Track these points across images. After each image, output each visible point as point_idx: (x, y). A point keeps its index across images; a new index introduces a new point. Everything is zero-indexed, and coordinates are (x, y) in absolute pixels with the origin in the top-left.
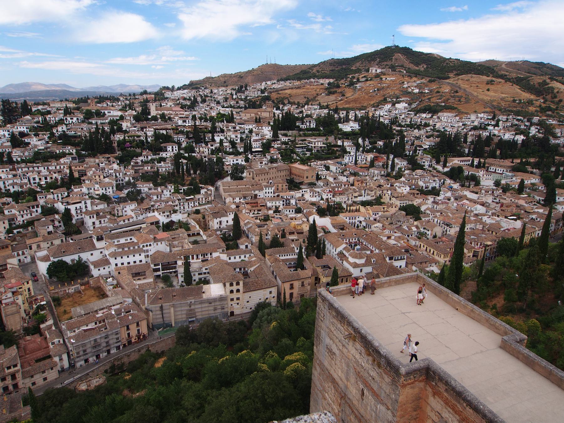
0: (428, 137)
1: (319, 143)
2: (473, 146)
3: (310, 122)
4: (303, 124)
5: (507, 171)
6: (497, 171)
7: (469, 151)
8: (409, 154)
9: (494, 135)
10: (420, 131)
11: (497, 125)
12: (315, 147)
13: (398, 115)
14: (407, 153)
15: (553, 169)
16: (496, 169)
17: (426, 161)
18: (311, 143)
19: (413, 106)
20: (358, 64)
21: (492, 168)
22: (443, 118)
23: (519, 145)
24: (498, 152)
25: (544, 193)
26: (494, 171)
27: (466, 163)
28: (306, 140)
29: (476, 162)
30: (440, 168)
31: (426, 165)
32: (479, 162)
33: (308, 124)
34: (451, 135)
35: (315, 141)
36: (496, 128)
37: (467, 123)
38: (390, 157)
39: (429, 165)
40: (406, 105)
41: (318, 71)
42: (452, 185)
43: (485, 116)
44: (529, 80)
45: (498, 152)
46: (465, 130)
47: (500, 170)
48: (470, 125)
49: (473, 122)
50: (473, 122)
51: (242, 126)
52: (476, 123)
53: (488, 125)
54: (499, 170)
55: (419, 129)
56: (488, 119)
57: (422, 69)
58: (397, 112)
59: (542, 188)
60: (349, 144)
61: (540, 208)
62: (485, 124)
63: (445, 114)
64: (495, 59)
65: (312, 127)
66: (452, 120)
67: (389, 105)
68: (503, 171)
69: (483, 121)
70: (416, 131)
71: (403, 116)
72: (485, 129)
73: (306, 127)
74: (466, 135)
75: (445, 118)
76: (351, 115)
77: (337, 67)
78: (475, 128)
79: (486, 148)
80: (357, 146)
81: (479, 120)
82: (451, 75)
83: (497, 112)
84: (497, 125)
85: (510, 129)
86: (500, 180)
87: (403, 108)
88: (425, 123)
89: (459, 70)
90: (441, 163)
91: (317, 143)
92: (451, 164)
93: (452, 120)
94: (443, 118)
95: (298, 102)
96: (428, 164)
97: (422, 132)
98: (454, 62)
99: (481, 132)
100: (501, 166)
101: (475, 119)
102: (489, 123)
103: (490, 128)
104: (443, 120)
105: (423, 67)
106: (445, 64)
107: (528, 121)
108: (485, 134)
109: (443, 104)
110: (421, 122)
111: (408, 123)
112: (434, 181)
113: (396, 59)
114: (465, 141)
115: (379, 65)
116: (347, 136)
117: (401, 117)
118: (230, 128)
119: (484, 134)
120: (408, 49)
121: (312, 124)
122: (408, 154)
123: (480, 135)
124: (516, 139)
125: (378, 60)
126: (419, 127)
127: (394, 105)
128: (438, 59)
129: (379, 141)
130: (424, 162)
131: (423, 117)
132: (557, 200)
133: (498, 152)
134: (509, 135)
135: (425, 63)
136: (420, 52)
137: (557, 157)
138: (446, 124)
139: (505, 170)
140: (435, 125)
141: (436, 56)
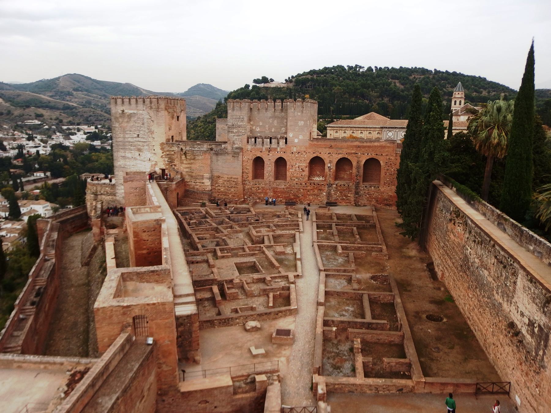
15: (11, 182)
25: (8, 207)
59: (5, 203)
137: (12, 170)
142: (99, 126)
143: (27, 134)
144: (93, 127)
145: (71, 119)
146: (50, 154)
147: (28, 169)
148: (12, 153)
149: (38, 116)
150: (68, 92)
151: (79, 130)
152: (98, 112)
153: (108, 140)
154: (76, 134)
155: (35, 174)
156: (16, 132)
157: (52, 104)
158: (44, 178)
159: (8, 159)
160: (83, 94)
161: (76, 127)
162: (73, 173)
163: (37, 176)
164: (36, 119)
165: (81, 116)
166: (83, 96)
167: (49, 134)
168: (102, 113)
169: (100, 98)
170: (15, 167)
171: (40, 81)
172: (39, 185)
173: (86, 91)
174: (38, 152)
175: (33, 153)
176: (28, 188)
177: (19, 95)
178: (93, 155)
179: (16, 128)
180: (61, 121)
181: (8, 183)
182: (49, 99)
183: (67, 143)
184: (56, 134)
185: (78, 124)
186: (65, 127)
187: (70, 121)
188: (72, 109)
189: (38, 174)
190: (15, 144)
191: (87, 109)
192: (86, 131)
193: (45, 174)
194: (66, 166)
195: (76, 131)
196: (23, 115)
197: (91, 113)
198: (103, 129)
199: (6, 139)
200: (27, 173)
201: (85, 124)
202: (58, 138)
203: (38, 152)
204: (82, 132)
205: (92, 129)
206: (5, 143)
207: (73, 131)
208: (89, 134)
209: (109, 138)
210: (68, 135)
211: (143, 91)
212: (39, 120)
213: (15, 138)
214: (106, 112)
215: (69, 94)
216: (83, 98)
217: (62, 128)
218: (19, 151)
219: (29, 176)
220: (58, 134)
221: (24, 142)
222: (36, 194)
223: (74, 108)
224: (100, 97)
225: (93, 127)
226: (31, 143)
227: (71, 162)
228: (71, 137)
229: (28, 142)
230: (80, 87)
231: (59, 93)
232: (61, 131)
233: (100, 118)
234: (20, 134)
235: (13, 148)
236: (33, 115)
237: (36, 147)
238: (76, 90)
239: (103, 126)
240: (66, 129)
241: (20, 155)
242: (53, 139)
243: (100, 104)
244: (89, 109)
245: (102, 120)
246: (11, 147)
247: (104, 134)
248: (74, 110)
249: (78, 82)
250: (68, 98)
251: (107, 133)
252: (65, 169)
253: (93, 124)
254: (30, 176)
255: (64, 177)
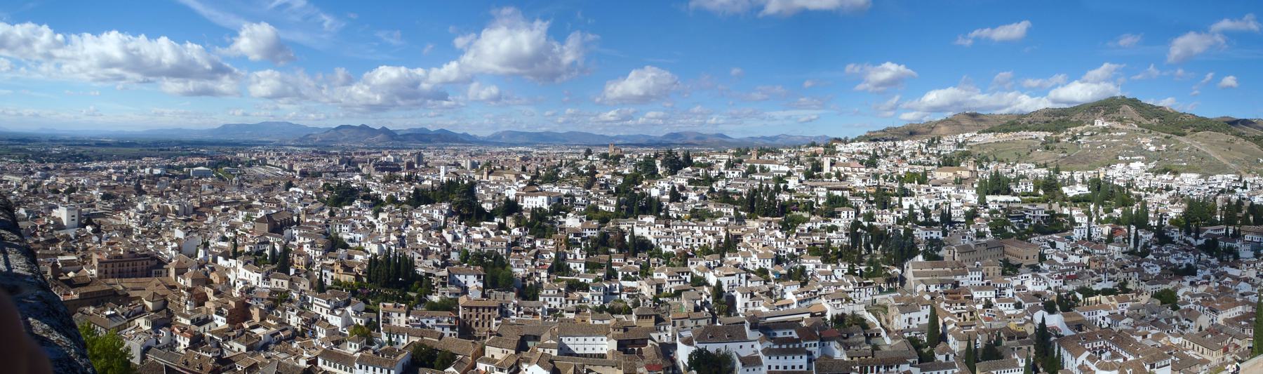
1: (1040, 212)
2: (1224, 212)
3: (1026, 184)
4: (1017, 187)
7: (1221, 218)
9: (1244, 199)
11: (1245, 187)
12: (1034, 217)
13: (1134, 177)
22: (1186, 179)
24: (1251, 218)
26: (1250, 240)
33: (1024, 187)
35: (1034, 208)
36: (1245, 190)
40: (1143, 165)
49: (1219, 184)
50: (1219, 184)
51: (938, 188)
52: (1223, 186)
53: (1236, 187)
56: (1234, 180)
70: (1158, 195)
72: (1233, 192)
78: (1222, 191)
84: (1245, 187)
87: (1139, 168)
88: (1167, 186)
90: (1193, 234)
91: (1036, 212)
94: (1186, 179)
99: (1230, 196)
103: (1238, 190)
108: (1234, 198)
109: (1185, 164)
110: (1162, 185)
111: (1147, 186)
116: (1076, 200)
117: (1138, 179)
118: (922, 190)
119: (1233, 198)
121: (1028, 188)
126: (1160, 191)
127: (1127, 163)
130: (1173, 234)
140: (1178, 188)
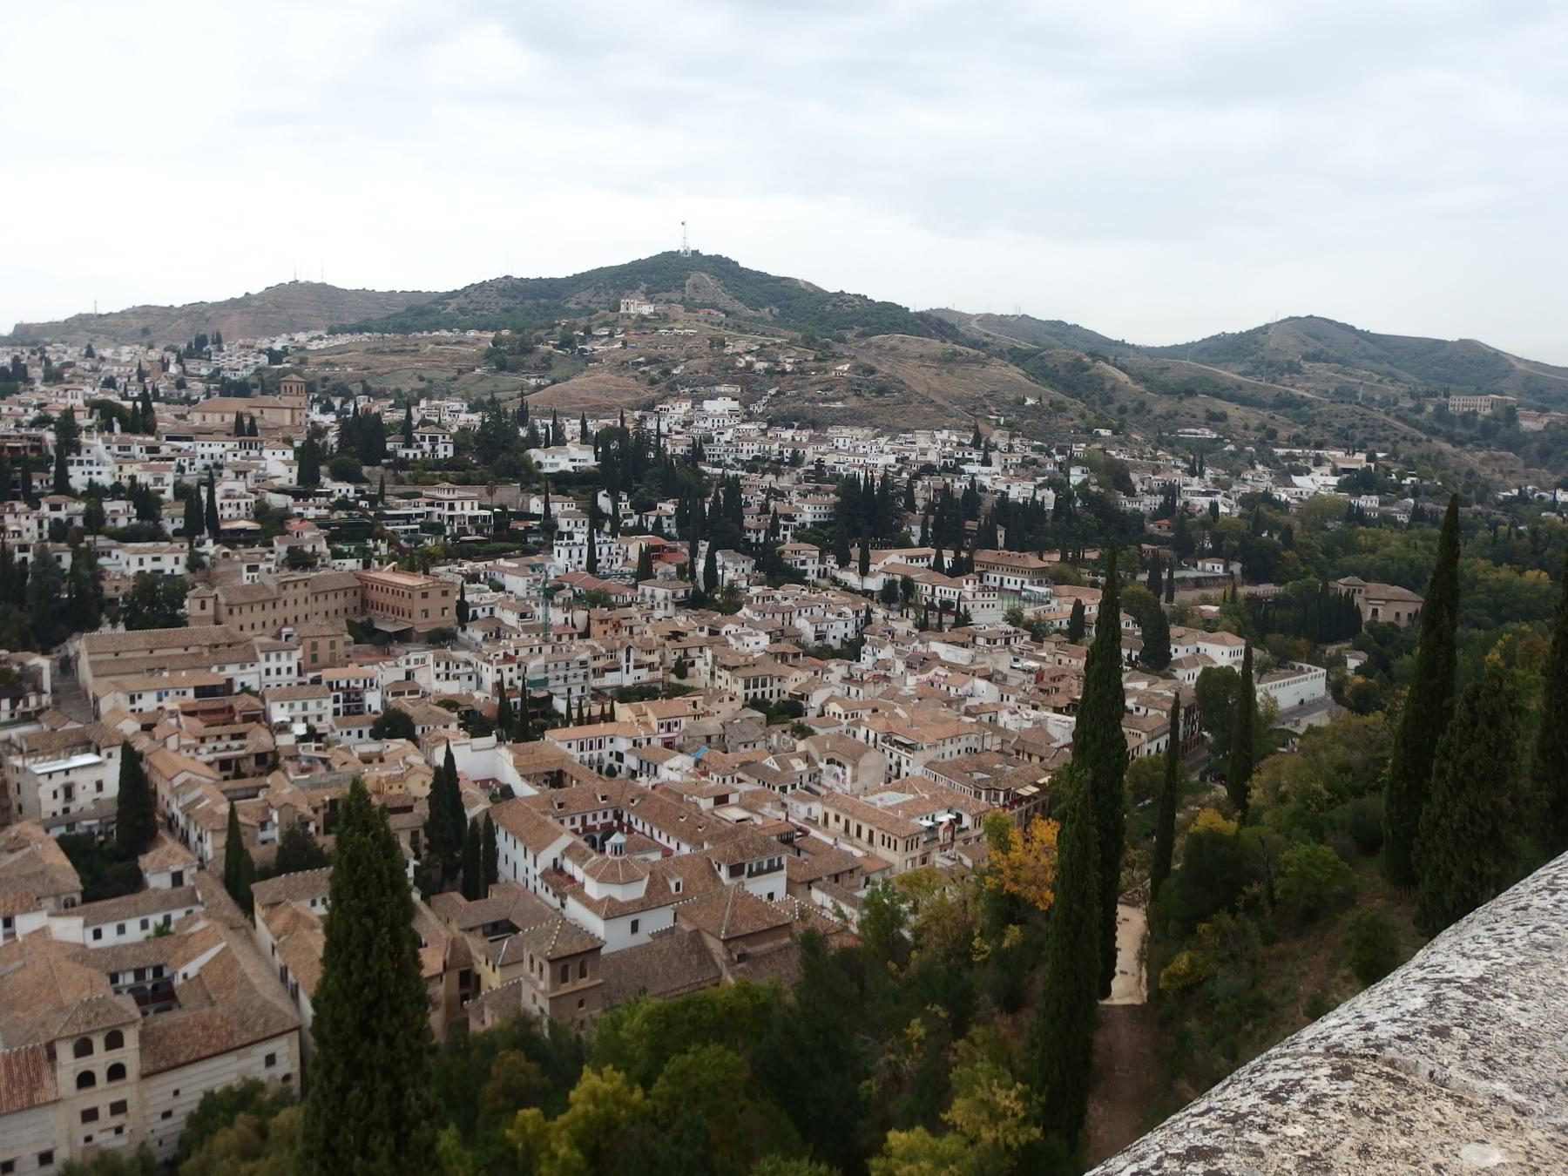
0: (803, 495)
1: (467, 505)
2: (931, 518)
3: (434, 440)
4: (408, 445)
5: (1032, 583)
6: (1006, 585)
7: (924, 531)
8: (758, 539)
9: (984, 489)
10: (780, 479)
12: (451, 518)
13: (714, 433)
14: (753, 537)
15: (1144, 577)
16: (1002, 580)
17: (808, 559)
18: (439, 505)
19: (758, 408)
20: (584, 297)
21: (992, 576)
22: (841, 440)
23: (1048, 517)
24: (1001, 533)
27: (920, 564)
28: (419, 495)
29: (948, 558)
30: (852, 578)
31: (810, 572)
32: (957, 559)
33: (427, 446)
34: (873, 480)
35: (451, 496)
37: (907, 454)
38: (701, 549)
39: (819, 571)
40: (735, 405)
41: (462, 310)
42: (894, 625)
43: (954, 438)
44: (1042, 358)
45: (1001, 533)
46: (905, 475)
47: (1012, 582)
48: (917, 461)
49: (924, 452)
54: (1012, 582)
55: (778, 474)
57: (770, 318)
58: (709, 424)
59: (1127, 625)
60: (566, 509)
61: (1138, 679)
62: (957, 459)
63: (846, 431)
64: (951, 308)
65: (441, 456)
66: (868, 449)
67: (684, 405)
68: (1023, 582)
69: (948, 449)
71: (728, 436)
73: (419, 456)
74: (910, 487)
75: (848, 441)
76: (572, 427)
77: (522, 303)
79: (969, 523)
80: (596, 519)
81: (939, 447)
82: (849, 335)
83: (982, 427)
84: (986, 462)
85: (1021, 471)
86: (1020, 609)
89: (868, 324)
90: (852, 565)
91: (458, 505)
92: (881, 565)
93: (868, 448)
94: (841, 440)
95: (398, 391)
96: (815, 567)
97: (785, 482)
98: (852, 301)
99: (948, 480)
100: (1015, 570)
101: (931, 446)
102: (967, 456)
104: (841, 447)
105: (771, 311)
106: (829, 308)
107: (1061, 451)
108: (959, 485)
110: (781, 453)
112: (840, 615)
113: (695, 287)
114: (911, 505)
115: (650, 297)
116: (563, 483)
119: (957, 485)
120: (727, 260)
121: (440, 448)
122: (754, 541)
123: (947, 485)
124: (1039, 498)
125: (644, 286)
126: (776, 467)
127: (698, 400)
128: (811, 294)
129: (664, 501)
130: (803, 563)
131: (785, 440)
132: (1175, 657)
133: (999, 533)
134: (1020, 489)
135: (775, 302)
136: (758, 273)
137: (1145, 546)
138: (851, 459)
139: (1027, 581)
141: (803, 286)
142: (1380, 455)
143: (1185, 460)
144: (1362, 456)
145: (1299, 430)
146: (1241, 516)
147: (1187, 550)
148: (1150, 503)
149: (1214, 418)
150: (1290, 363)
151: (1319, 462)
152: (1376, 415)
153: (1405, 496)
154: (1308, 472)
155: (1200, 564)
156: (1160, 453)
157: (1247, 393)
158: (1223, 578)
159: (1138, 516)
160: (1329, 370)
161: (1313, 453)
162: (1306, 574)
163: (1203, 570)
164: (1207, 425)
165: (1324, 425)
166: (1331, 374)
167: (1235, 467)
168: (1389, 420)
169: (1380, 381)
170: (1151, 539)
171: (1213, 338)
172: (1213, 593)
173: (1339, 361)
174: (1214, 506)
175: (1198, 508)
176: (1183, 596)
177: (1163, 370)
178: (1362, 533)
179: (1160, 443)
180: (1272, 434)
181: (1134, 578)
182: (1241, 378)
183: (1282, 494)
184: (1254, 468)
185: (1319, 446)
186: (1280, 451)
187: (1296, 436)
188: (1299, 407)
189: (1208, 566)
190: (1157, 480)
191: (1345, 407)
192: (1341, 465)
193: (1226, 568)
194: (1289, 554)
195: (1310, 464)
196: (1176, 414)
197: (1356, 420)
198: (1390, 464)
199: (1136, 467)
200: (1180, 558)
201: (1339, 447)
202: (1259, 479)
203: (1214, 506)
204: (1326, 469)
205: (1360, 460)
206: (1134, 477)
207: (1301, 463)
208: (1345, 476)
209: (1406, 489)
210: (1286, 472)
211: (1515, 363)
212: (1213, 430)
213: (1158, 466)
214: (1398, 417)
215: (1292, 368)
216: (1329, 380)
217: (1271, 454)
218: (1166, 499)
219: (1182, 568)
220: (1260, 468)
221: (1178, 477)
222: (1206, 616)
223: (1305, 404)
224: (1377, 377)
225: (1362, 456)
226: (1196, 484)
227: (1301, 544)
228: (1295, 479)
229: (1188, 479)
230: (1322, 351)
231: (1263, 367)
232: (1270, 461)
233: (1382, 434)
234: (1170, 458)
235: (1151, 492)
236: (1201, 415)
237: (1207, 494)
238: (1314, 357)
239: (1393, 456)
240: (1284, 457)
241: (1167, 510)
242: (1244, 480)
243: (1378, 397)
244: (1350, 407)
245: (1386, 439)
246: (1145, 488)
247: (1394, 477)
248: (1306, 408)
249: (1318, 338)
250: (1286, 379)
251: (1401, 476)
252: (1284, 559)
253: (1361, 447)
254: (1187, 569)
255: (1279, 583)
